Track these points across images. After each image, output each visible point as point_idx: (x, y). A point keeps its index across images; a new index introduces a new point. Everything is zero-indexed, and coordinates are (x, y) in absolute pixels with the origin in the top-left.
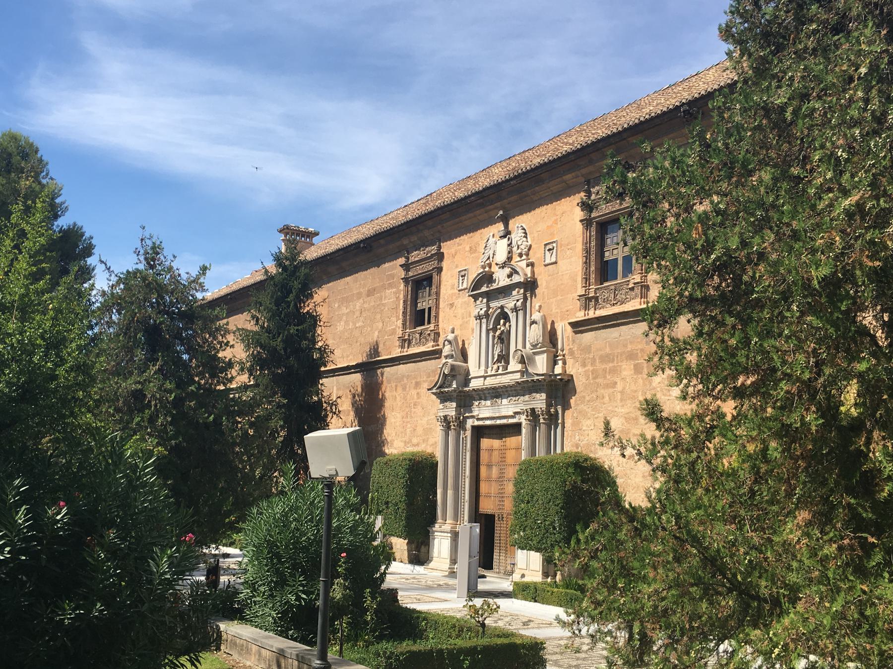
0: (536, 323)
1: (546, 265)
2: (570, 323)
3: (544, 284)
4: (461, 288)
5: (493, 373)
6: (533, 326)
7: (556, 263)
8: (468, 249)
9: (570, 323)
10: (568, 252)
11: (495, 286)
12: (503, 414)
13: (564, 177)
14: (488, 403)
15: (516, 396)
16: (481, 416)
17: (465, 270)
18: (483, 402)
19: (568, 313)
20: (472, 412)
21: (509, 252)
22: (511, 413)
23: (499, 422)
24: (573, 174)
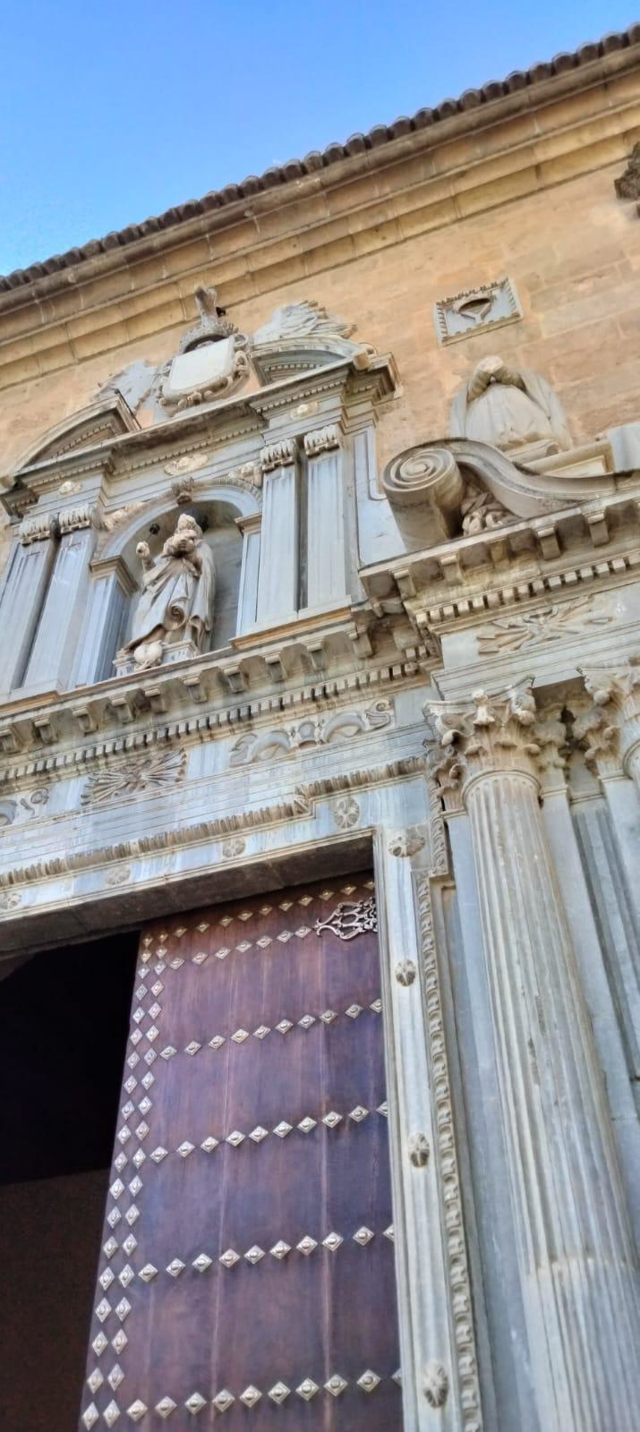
10: (581, 287)
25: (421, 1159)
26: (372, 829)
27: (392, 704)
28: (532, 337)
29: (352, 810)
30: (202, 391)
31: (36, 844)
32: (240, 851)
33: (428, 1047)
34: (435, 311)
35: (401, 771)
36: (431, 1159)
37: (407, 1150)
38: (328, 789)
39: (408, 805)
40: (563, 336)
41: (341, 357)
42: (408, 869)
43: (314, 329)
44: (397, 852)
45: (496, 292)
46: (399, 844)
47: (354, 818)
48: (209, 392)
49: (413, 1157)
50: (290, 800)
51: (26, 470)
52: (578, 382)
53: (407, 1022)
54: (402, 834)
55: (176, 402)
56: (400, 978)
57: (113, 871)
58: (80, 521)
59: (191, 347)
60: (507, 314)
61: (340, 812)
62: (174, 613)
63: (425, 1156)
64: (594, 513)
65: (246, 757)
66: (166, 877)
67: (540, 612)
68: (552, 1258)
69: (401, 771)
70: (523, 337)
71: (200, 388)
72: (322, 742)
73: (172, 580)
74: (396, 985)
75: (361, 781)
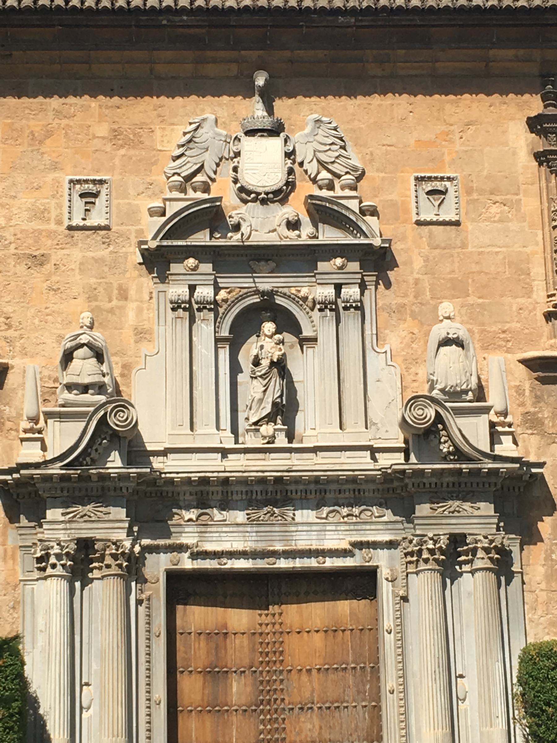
0: (462, 346)
1: (419, 223)
2: (524, 362)
3: (418, 263)
4: (77, 221)
5: (259, 443)
6: (443, 349)
7: (457, 223)
8: (103, 130)
9: (524, 362)
10: (494, 209)
11: (234, 239)
12: (302, 544)
13: (492, 52)
14: (240, 516)
15: (351, 505)
16: (209, 547)
17: (101, 182)
18: (217, 515)
19: (508, 336)
20: (168, 535)
21: (291, 171)
22: (344, 545)
23: (283, 564)
24: (521, 52)
25: (392, 692)
26: (377, 567)
27: (386, 503)
28: (464, 245)
29: (370, 555)
30: (267, 194)
31: (229, 534)
32: (324, 563)
33: (396, 658)
34: (413, 182)
35: (391, 545)
36: (395, 692)
37: (388, 688)
38: (360, 545)
39: (391, 559)
40: (480, 253)
41: (366, 236)
42: (391, 588)
43: (337, 157)
44: (387, 579)
45: (448, 184)
46: (388, 576)
47: (371, 558)
48: (271, 196)
49: (390, 691)
50: (348, 547)
51: (165, 243)
52: (480, 301)
53: (389, 647)
54: (388, 571)
55: (249, 193)
56: (387, 631)
57: (271, 560)
58: (208, 304)
59: (251, 133)
60: (454, 218)
61: (365, 555)
62: (274, 404)
63: (393, 691)
64: (485, 468)
65: (323, 514)
66: (294, 568)
67: (454, 495)
68: (434, 729)
69: (391, 545)
70: (458, 243)
71: (267, 189)
72: (356, 516)
73: (273, 380)
74: (386, 633)
75: (375, 545)
